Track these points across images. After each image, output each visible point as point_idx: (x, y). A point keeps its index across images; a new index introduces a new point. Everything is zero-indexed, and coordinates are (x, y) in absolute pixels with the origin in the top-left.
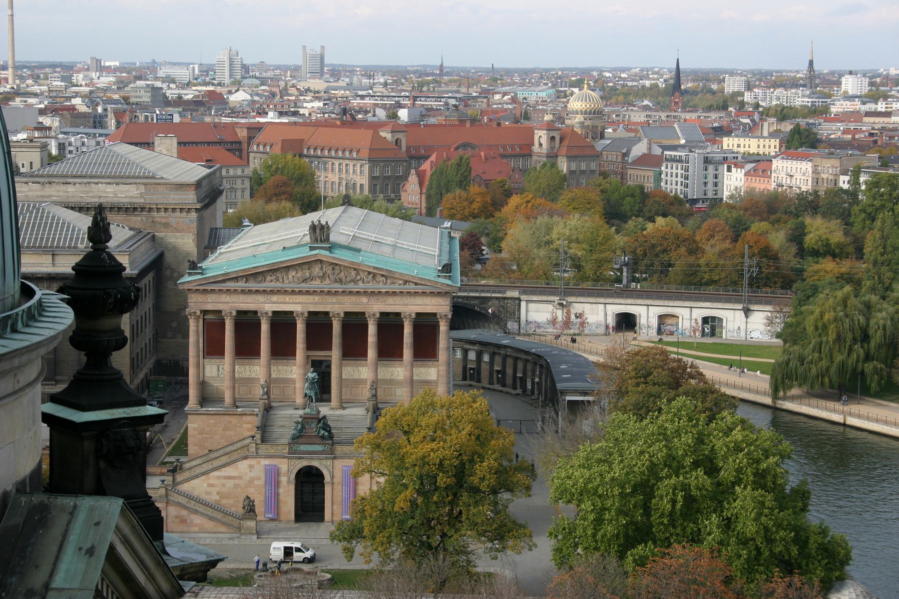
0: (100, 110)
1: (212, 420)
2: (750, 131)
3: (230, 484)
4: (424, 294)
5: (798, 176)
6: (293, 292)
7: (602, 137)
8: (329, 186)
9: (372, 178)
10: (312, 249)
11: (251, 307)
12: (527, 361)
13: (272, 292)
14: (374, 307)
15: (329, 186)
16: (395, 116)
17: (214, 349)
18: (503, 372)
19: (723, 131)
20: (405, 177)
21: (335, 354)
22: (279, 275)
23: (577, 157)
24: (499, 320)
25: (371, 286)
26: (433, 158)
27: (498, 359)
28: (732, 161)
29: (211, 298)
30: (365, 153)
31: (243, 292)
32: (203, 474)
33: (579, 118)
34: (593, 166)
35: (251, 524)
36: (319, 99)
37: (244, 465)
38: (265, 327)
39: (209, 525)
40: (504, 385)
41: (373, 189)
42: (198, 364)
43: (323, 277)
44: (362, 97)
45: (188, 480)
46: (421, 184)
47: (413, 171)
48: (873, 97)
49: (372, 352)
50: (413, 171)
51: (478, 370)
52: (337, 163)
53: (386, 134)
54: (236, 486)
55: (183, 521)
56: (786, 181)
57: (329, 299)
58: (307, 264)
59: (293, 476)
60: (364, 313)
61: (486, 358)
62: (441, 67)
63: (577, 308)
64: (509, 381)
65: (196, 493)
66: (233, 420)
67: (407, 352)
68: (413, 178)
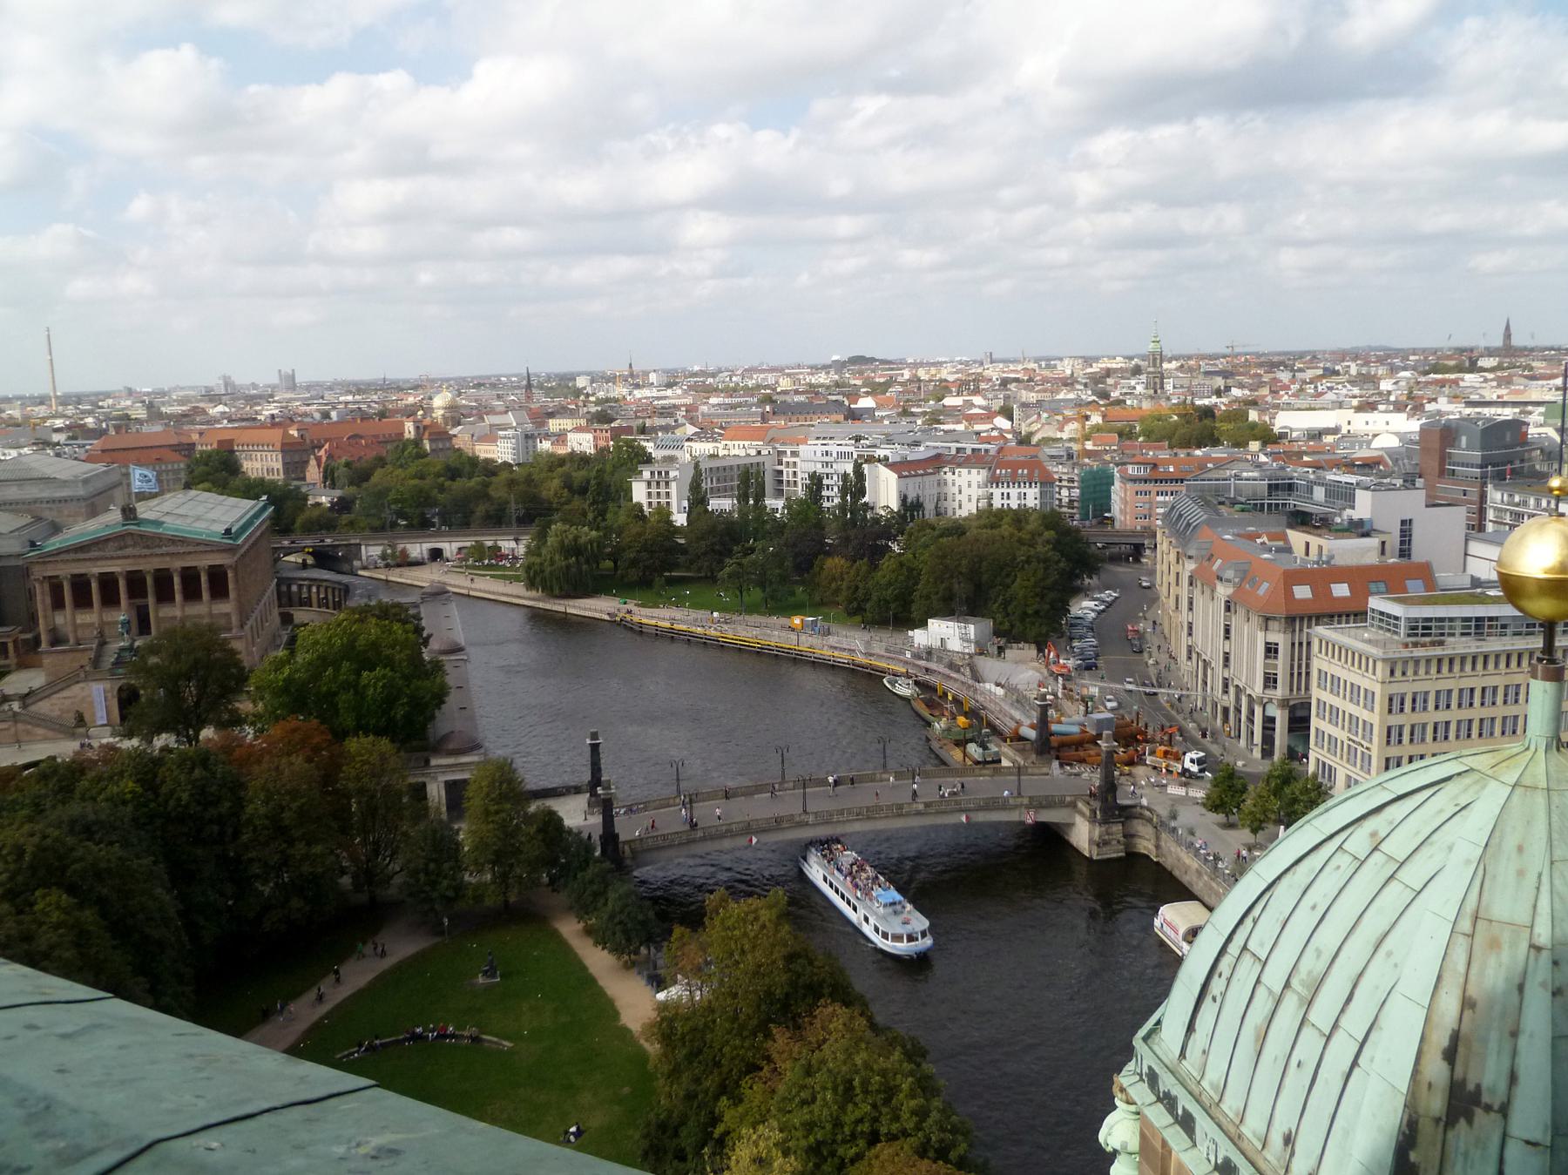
0: (104, 425)
1: (61, 657)
2: (572, 414)
3: (68, 702)
4: (212, 551)
5: (584, 444)
6: (112, 558)
7: (459, 424)
8: (255, 471)
9: (285, 464)
10: (124, 525)
11: (82, 571)
12: (340, 590)
13: (97, 559)
14: (177, 564)
15: (255, 471)
16: (326, 415)
17: (58, 604)
18: (326, 598)
19: (551, 415)
20: (307, 462)
21: (151, 600)
22: (100, 546)
23: (437, 439)
24: (347, 559)
25: (172, 549)
26: (327, 446)
27: (322, 590)
28: (547, 436)
29: (49, 566)
30: (278, 446)
31: (74, 560)
32: (46, 697)
33: (441, 412)
34: (448, 445)
35: (82, 730)
36: (276, 407)
37: (76, 689)
38: (94, 586)
39: (50, 734)
40: (328, 608)
41: (286, 471)
42: (45, 617)
43: (134, 546)
44: (308, 405)
45: (33, 703)
46: (319, 466)
47: (312, 457)
48: (669, 385)
49: (178, 597)
50: (312, 457)
51: (310, 598)
52: (259, 454)
53: (294, 433)
54: (72, 703)
55: (28, 732)
56: (577, 449)
57: (142, 561)
58: (120, 537)
59: (115, 693)
60: (168, 569)
61: (314, 589)
62: (384, 380)
63: (400, 547)
64: (331, 604)
65: (42, 711)
66: (79, 655)
67: (206, 595)
68: (313, 462)
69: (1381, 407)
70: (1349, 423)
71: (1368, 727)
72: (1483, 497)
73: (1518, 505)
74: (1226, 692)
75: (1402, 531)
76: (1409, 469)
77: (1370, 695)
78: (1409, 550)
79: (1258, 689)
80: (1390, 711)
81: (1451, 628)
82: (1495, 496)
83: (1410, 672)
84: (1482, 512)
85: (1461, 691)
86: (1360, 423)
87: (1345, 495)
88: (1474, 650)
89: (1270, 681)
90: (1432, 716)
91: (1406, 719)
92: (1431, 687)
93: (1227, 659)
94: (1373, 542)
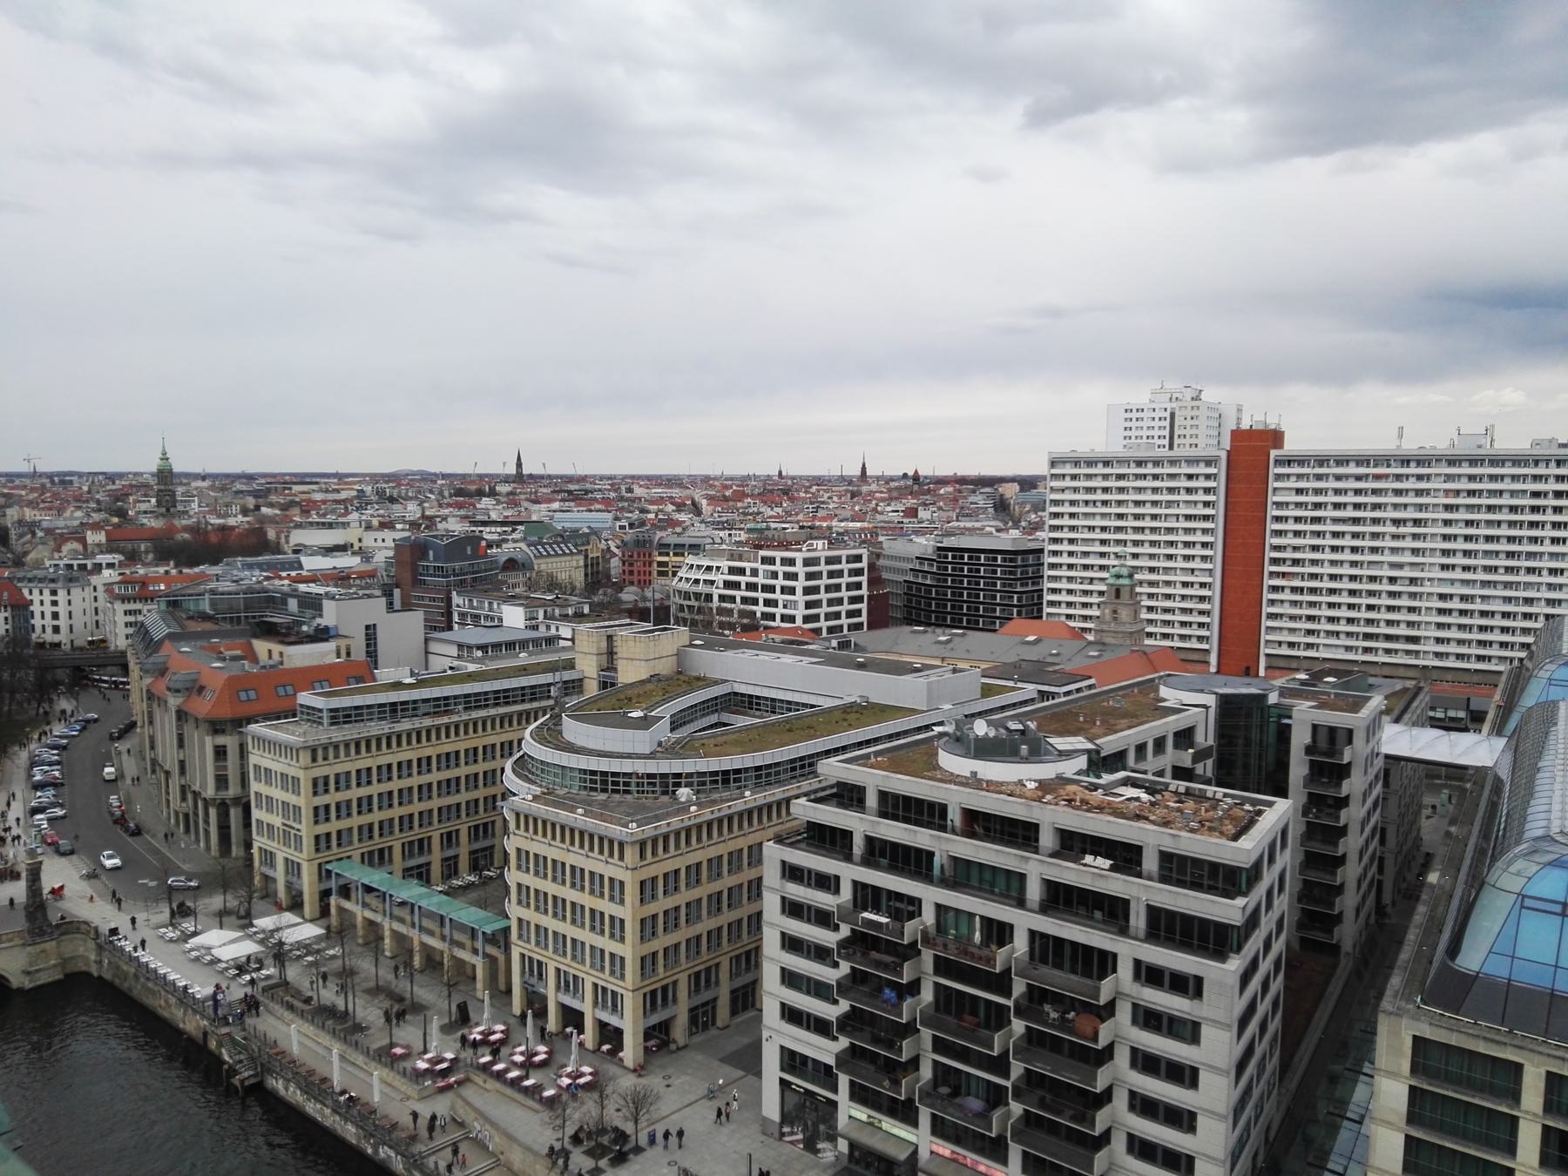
69: (399, 526)
70: (360, 540)
71: (297, 809)
72: (449, 600)
73: (476, 609)
74: (184, 799)
75: (367, 634)
76: (386, 580)
77: (296, 780)
78: (376, 651)
79: (210, 792)
80: (315, 794)
81: (369, 714)
82: (457, 599)
83: (331, 755)
84: (449, 614)
85: (379, 767)
86: (369, 540)
87: (312, 604)
88: (387, 731)
89: (222, 781)
90: (355, 793)
91: (332, 798)
92: (352, 767)
93: (182, 764)
94: (330, 646)
